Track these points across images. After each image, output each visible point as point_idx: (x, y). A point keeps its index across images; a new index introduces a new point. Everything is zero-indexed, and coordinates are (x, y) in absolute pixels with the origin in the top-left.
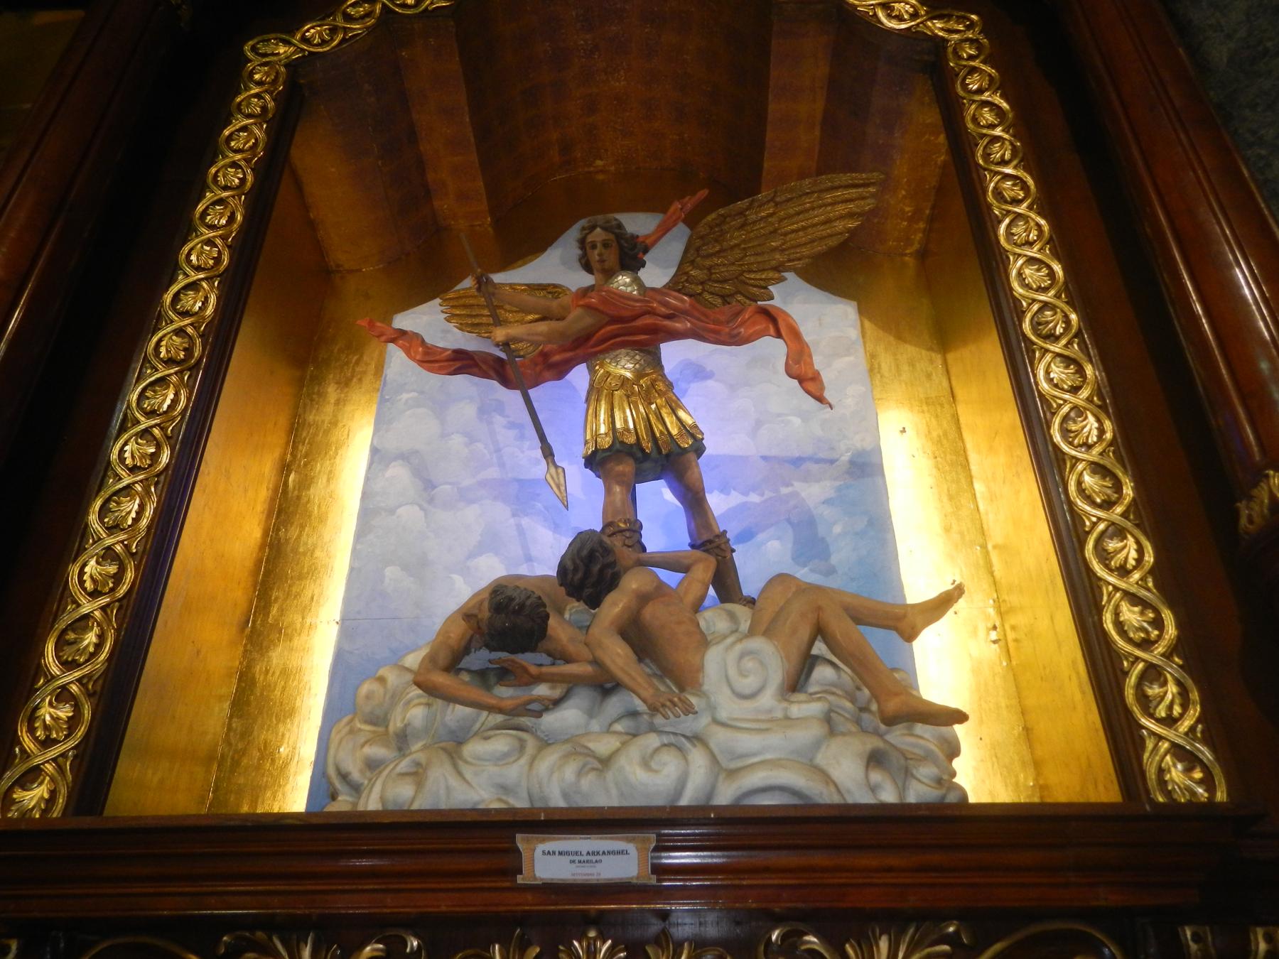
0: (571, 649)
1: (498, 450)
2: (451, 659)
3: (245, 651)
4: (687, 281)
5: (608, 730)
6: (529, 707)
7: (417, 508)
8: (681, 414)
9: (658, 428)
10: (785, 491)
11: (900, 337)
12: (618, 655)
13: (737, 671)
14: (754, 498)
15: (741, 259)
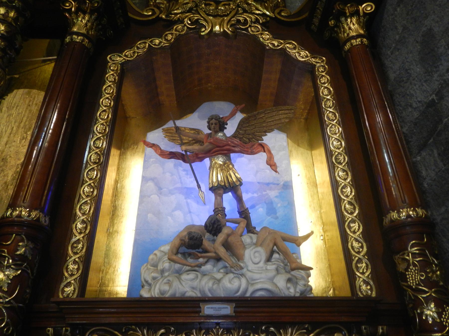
1: (180, 178)
5: (219, 271)
7: (156, 196)
8: (236, 174)
9: (230, 179)
10: (264, 193)
12: (222, 251)
13: (253, 257)
14: (255, 195)
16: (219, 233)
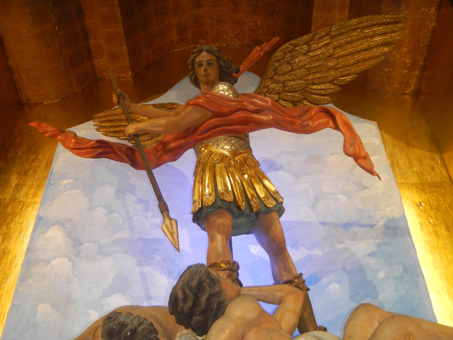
1: (129, 218)
4: (267, 92)
7: (66, 260)
8: (266, 183)
10: (339, 246)
11: (408, 143)
14: (317, 252)
15: (307, 75)
16: (216, 318)
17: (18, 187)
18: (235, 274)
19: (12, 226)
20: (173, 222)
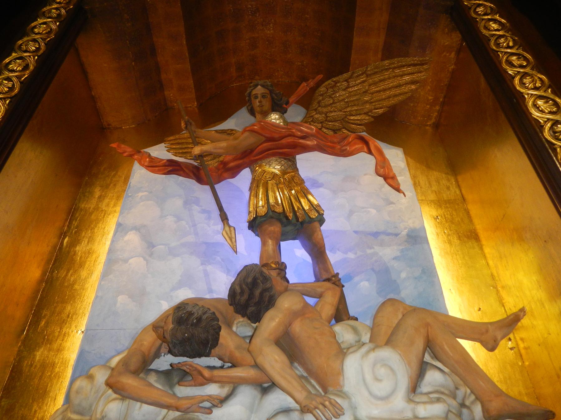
0: (237, 354)
1: (194, 225)
2: (140, 364)
3: (19, 351)
4: (312, 121)
6: (201, 405)
7: (142, 259)
8: (310, 197)
10: (369, 251)
11: (429, 167)
12: (274, 360)
14: (351, 255)
15: (346, 108)
16: (267, 309)
17: (101, 198)
18: (283, 273)
19: (96, 230)
20: (232, 229)
